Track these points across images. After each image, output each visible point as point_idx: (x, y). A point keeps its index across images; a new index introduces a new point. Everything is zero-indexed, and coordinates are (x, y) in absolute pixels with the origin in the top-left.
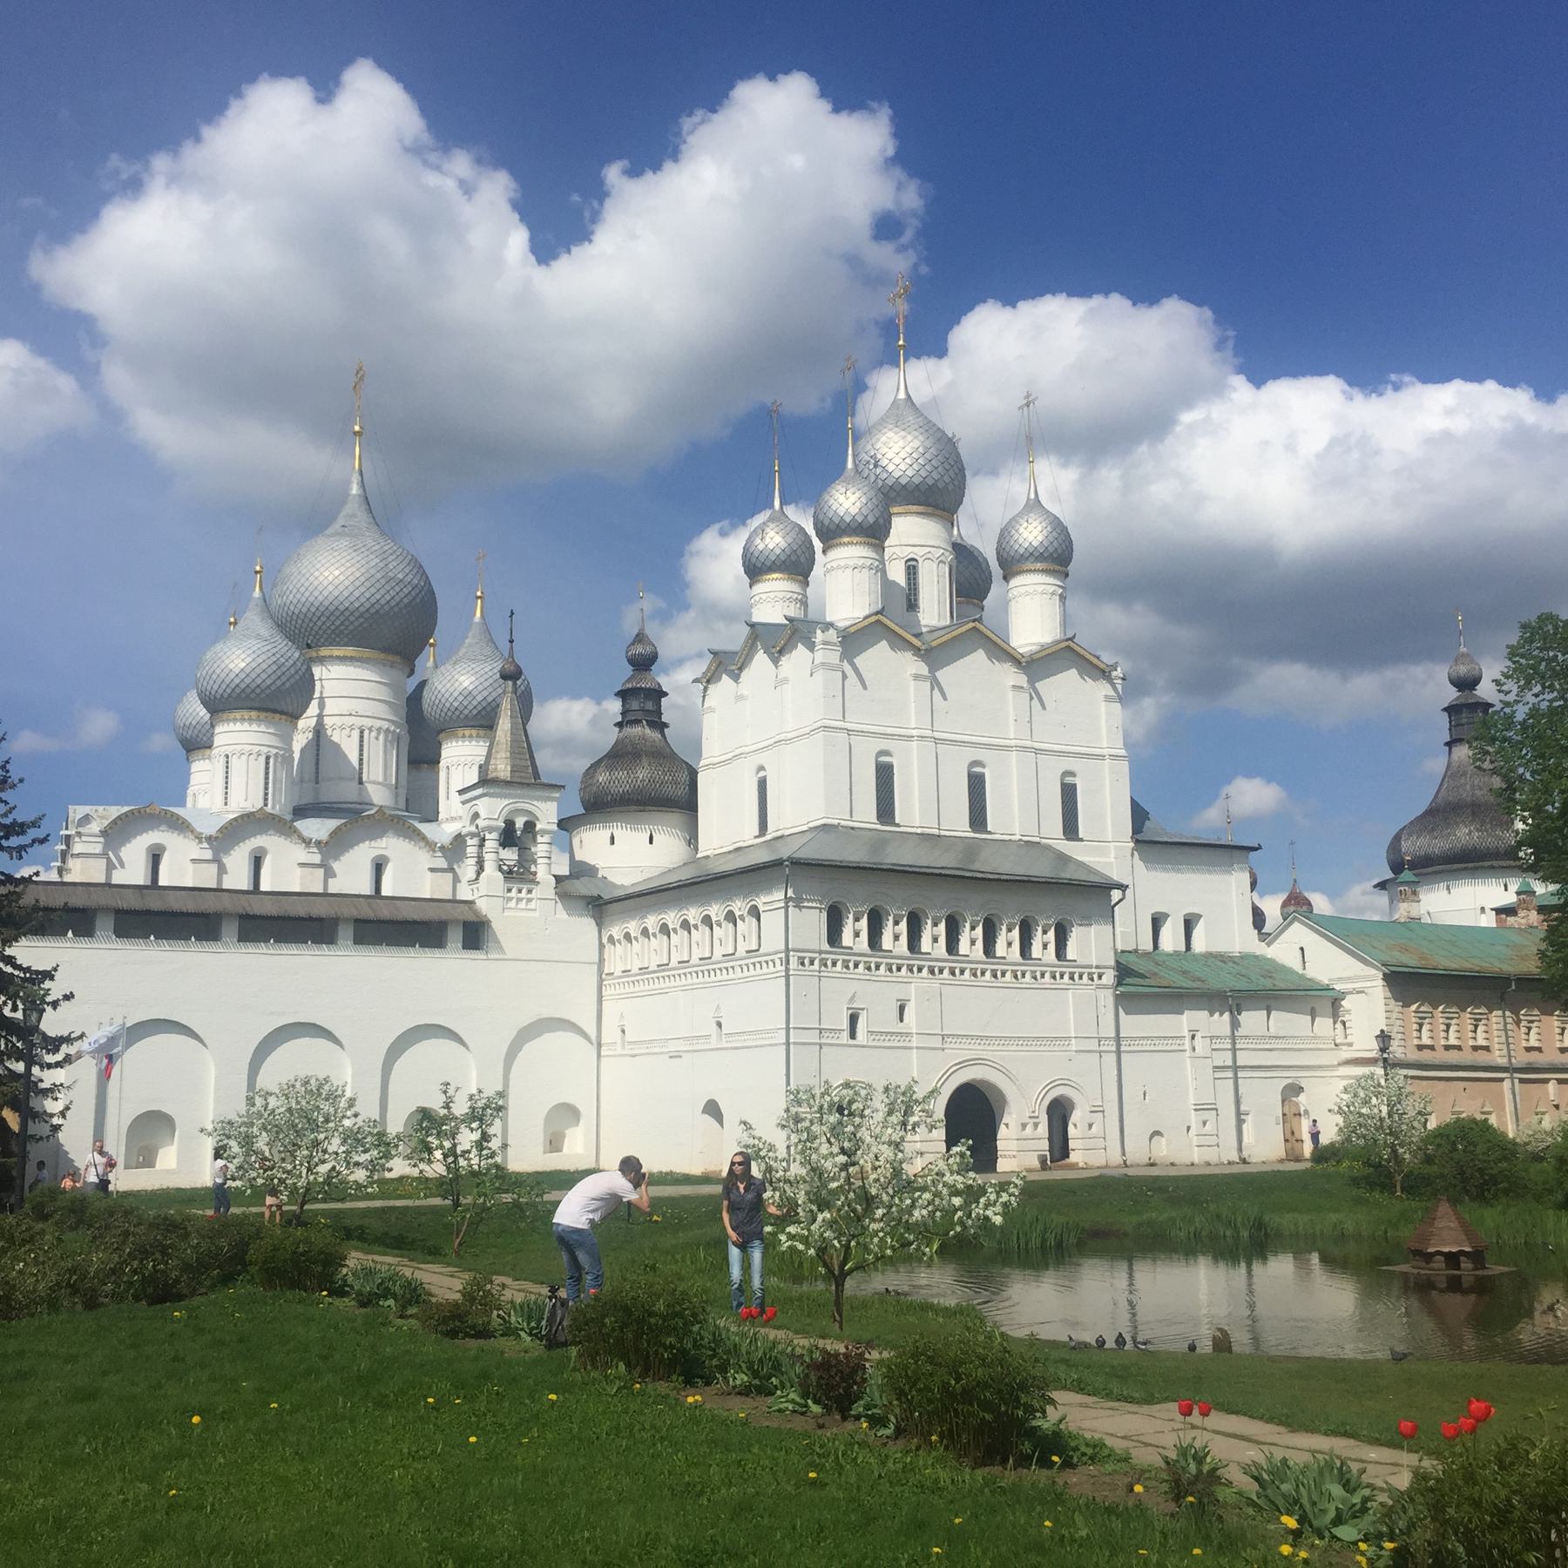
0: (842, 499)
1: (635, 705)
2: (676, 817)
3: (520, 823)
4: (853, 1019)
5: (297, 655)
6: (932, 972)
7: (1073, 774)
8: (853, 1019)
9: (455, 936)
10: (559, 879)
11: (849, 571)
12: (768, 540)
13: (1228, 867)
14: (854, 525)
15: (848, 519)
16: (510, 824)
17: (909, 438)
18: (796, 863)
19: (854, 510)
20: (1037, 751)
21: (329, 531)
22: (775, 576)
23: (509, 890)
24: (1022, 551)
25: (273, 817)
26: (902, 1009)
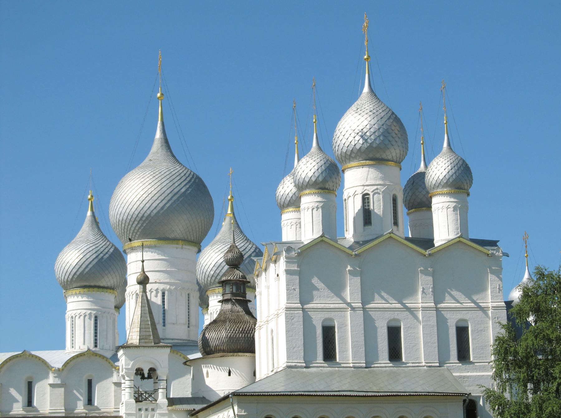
0: (304, 168)
1: (228, 289)
2: (241, 360)
5: (111, 250)
7: (466, 321)
10: (172, 402)
11: (310, 210)
12: (285, 188)
14: (311, 183)
15: (307, 180)
17: (363, 119)
18: (236, 394)
19: (310, 174)
20: (437, 309)
21: (141, 166)
22: (291, 209)
23: (140, 410)
24: (434, 182)
25: (95, 354)
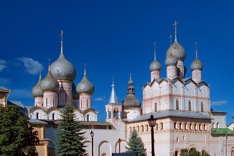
3: (116, 110)
4: (177, 139)
6: (188, 132)
8: (177, 139)
9: (108, 127)
13: (223, 115)
16: (115, 110)
26: (183, 137)
